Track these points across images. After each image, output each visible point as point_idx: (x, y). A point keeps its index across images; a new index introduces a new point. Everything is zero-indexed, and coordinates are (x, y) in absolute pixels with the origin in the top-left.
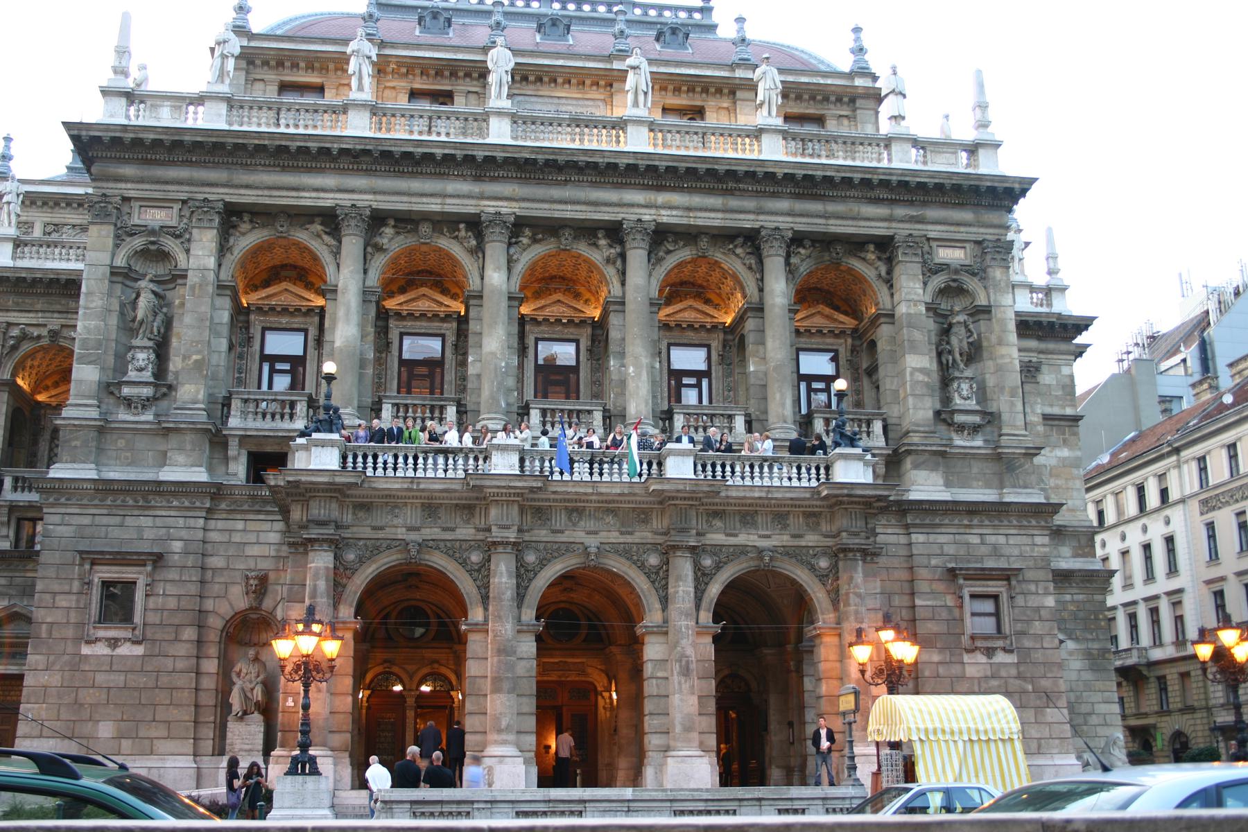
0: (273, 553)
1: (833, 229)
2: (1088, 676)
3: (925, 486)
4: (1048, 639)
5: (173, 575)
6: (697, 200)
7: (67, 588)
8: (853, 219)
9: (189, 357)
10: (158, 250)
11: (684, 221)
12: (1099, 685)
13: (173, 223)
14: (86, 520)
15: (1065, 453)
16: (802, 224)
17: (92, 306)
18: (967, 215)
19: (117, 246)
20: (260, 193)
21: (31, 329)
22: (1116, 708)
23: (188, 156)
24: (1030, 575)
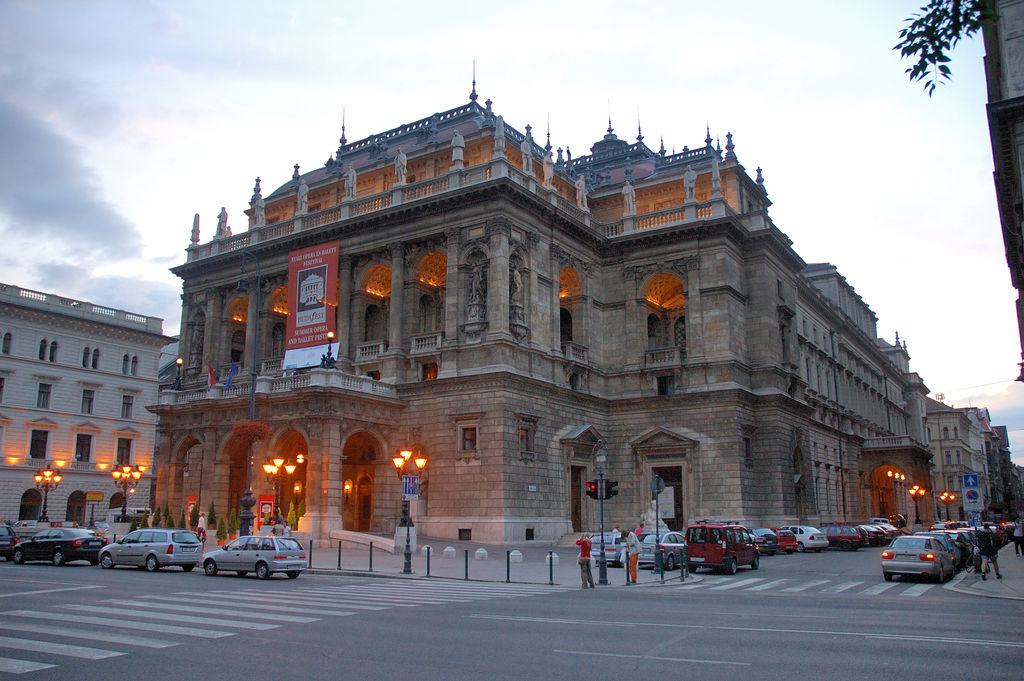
1: (419, 236)
2: (721, 460)
3: (447, 371)
4: (497, 451)
6: (363, 238)
8: (425, 228)
11: (359, 250)
12: (727, 466)
15: (717, 312)
16: (405, 238)
18: (480, 209)
22: (738, 481)
24: (492, 415)
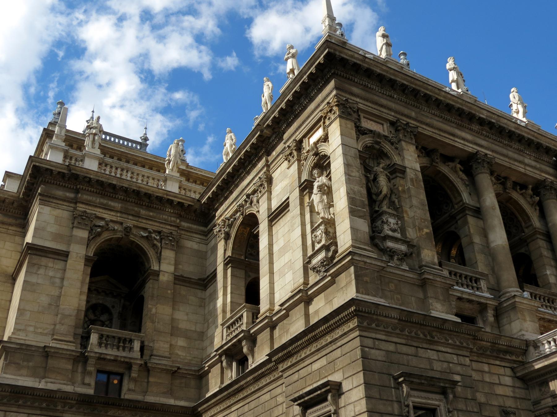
0: (511, 394)
5: (461, 405)
7: (390, 409)
9: (422, 229)
10: (379, 150)
13: (386, 134)
14: (391, 347)
17: (353, 174)
19: (358, 139)
20: (434, 131)
21: (111, 225)
23: (392, 93)
